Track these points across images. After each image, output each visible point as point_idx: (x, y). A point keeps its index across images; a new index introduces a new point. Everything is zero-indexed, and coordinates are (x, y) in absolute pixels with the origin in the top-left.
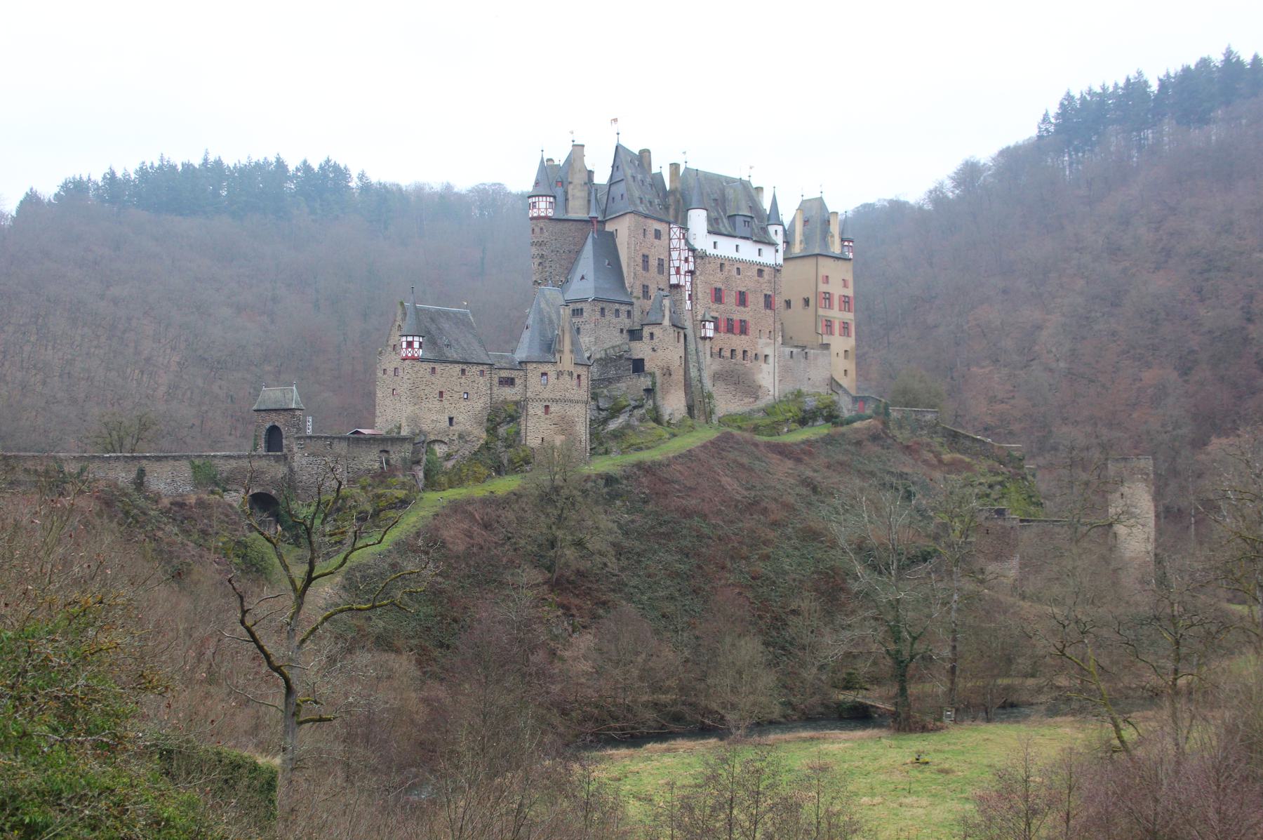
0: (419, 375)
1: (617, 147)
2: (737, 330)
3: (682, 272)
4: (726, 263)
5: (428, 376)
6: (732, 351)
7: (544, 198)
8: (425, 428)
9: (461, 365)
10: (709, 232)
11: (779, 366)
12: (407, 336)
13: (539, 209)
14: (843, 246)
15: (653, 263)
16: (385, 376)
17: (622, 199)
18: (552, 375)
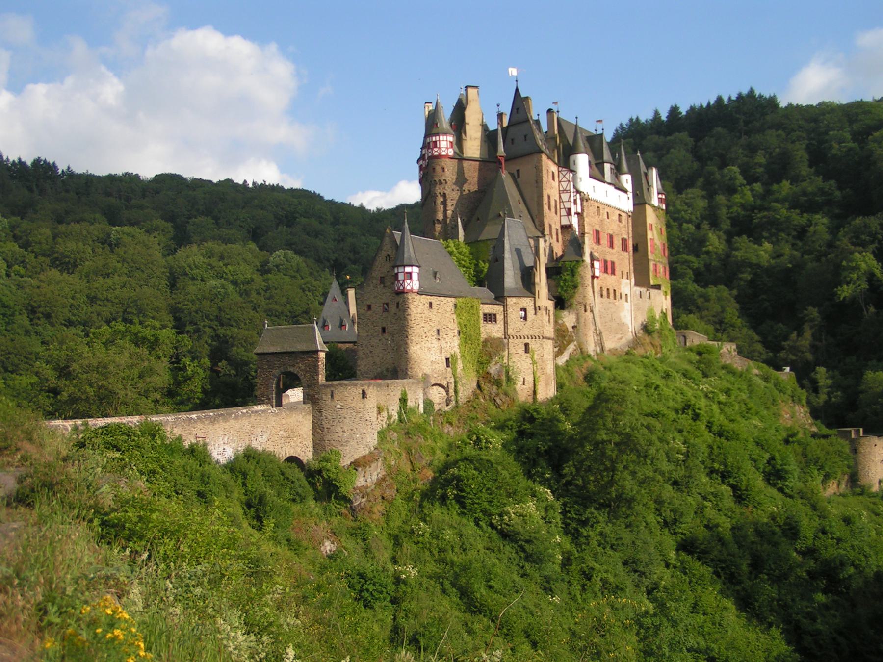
0: (419, 311)
1: (517, 90)
2: (609, 271)
3: (573, 213)
4: (601, 207)
5: (426, 312)
6: (608, 289)
7: (445, 138)
8: (428, 371)
9: (453, 299)
10: (590, 177)
11: (634, 305)
12: (404, 266)
13: (440, 148)
14: (659, 198)
15: (553, 203)
16: (369, 313)
17: (525, 140)
18: (531, 312)
